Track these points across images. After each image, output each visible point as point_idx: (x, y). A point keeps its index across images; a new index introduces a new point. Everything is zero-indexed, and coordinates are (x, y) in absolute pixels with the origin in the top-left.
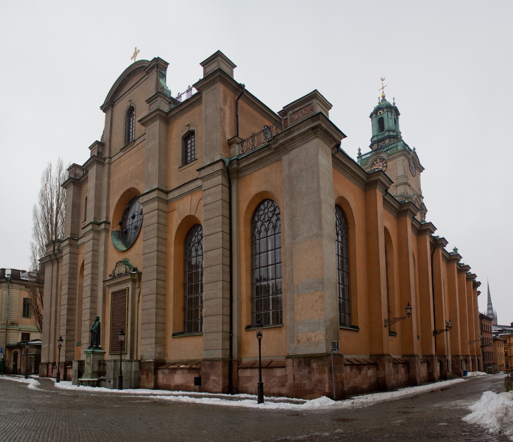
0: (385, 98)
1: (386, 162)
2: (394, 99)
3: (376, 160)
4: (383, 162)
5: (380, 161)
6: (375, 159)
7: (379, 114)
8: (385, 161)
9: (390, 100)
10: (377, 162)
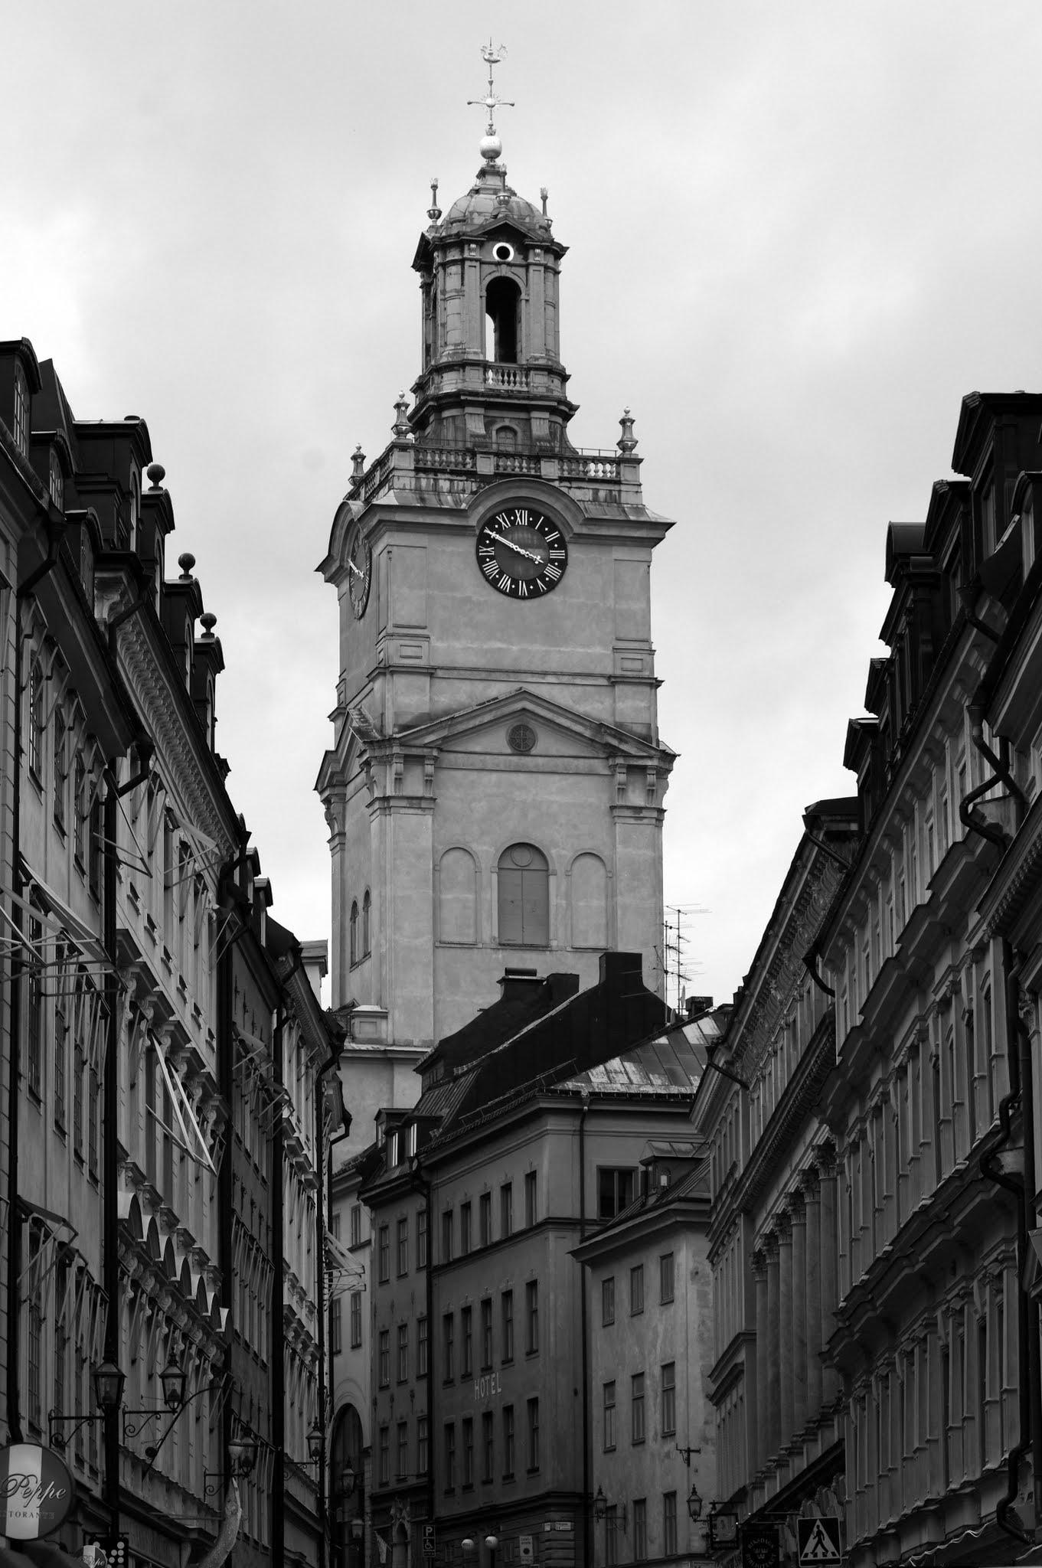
1: (562, 544)
2: (544, 198)
3: (510, 512)
4: (550, 538)
5: (531, 524)
6: (509, 505)
7: (497, 258)
8: (555, 535)
9: (525, 186)
10: (513, 523)
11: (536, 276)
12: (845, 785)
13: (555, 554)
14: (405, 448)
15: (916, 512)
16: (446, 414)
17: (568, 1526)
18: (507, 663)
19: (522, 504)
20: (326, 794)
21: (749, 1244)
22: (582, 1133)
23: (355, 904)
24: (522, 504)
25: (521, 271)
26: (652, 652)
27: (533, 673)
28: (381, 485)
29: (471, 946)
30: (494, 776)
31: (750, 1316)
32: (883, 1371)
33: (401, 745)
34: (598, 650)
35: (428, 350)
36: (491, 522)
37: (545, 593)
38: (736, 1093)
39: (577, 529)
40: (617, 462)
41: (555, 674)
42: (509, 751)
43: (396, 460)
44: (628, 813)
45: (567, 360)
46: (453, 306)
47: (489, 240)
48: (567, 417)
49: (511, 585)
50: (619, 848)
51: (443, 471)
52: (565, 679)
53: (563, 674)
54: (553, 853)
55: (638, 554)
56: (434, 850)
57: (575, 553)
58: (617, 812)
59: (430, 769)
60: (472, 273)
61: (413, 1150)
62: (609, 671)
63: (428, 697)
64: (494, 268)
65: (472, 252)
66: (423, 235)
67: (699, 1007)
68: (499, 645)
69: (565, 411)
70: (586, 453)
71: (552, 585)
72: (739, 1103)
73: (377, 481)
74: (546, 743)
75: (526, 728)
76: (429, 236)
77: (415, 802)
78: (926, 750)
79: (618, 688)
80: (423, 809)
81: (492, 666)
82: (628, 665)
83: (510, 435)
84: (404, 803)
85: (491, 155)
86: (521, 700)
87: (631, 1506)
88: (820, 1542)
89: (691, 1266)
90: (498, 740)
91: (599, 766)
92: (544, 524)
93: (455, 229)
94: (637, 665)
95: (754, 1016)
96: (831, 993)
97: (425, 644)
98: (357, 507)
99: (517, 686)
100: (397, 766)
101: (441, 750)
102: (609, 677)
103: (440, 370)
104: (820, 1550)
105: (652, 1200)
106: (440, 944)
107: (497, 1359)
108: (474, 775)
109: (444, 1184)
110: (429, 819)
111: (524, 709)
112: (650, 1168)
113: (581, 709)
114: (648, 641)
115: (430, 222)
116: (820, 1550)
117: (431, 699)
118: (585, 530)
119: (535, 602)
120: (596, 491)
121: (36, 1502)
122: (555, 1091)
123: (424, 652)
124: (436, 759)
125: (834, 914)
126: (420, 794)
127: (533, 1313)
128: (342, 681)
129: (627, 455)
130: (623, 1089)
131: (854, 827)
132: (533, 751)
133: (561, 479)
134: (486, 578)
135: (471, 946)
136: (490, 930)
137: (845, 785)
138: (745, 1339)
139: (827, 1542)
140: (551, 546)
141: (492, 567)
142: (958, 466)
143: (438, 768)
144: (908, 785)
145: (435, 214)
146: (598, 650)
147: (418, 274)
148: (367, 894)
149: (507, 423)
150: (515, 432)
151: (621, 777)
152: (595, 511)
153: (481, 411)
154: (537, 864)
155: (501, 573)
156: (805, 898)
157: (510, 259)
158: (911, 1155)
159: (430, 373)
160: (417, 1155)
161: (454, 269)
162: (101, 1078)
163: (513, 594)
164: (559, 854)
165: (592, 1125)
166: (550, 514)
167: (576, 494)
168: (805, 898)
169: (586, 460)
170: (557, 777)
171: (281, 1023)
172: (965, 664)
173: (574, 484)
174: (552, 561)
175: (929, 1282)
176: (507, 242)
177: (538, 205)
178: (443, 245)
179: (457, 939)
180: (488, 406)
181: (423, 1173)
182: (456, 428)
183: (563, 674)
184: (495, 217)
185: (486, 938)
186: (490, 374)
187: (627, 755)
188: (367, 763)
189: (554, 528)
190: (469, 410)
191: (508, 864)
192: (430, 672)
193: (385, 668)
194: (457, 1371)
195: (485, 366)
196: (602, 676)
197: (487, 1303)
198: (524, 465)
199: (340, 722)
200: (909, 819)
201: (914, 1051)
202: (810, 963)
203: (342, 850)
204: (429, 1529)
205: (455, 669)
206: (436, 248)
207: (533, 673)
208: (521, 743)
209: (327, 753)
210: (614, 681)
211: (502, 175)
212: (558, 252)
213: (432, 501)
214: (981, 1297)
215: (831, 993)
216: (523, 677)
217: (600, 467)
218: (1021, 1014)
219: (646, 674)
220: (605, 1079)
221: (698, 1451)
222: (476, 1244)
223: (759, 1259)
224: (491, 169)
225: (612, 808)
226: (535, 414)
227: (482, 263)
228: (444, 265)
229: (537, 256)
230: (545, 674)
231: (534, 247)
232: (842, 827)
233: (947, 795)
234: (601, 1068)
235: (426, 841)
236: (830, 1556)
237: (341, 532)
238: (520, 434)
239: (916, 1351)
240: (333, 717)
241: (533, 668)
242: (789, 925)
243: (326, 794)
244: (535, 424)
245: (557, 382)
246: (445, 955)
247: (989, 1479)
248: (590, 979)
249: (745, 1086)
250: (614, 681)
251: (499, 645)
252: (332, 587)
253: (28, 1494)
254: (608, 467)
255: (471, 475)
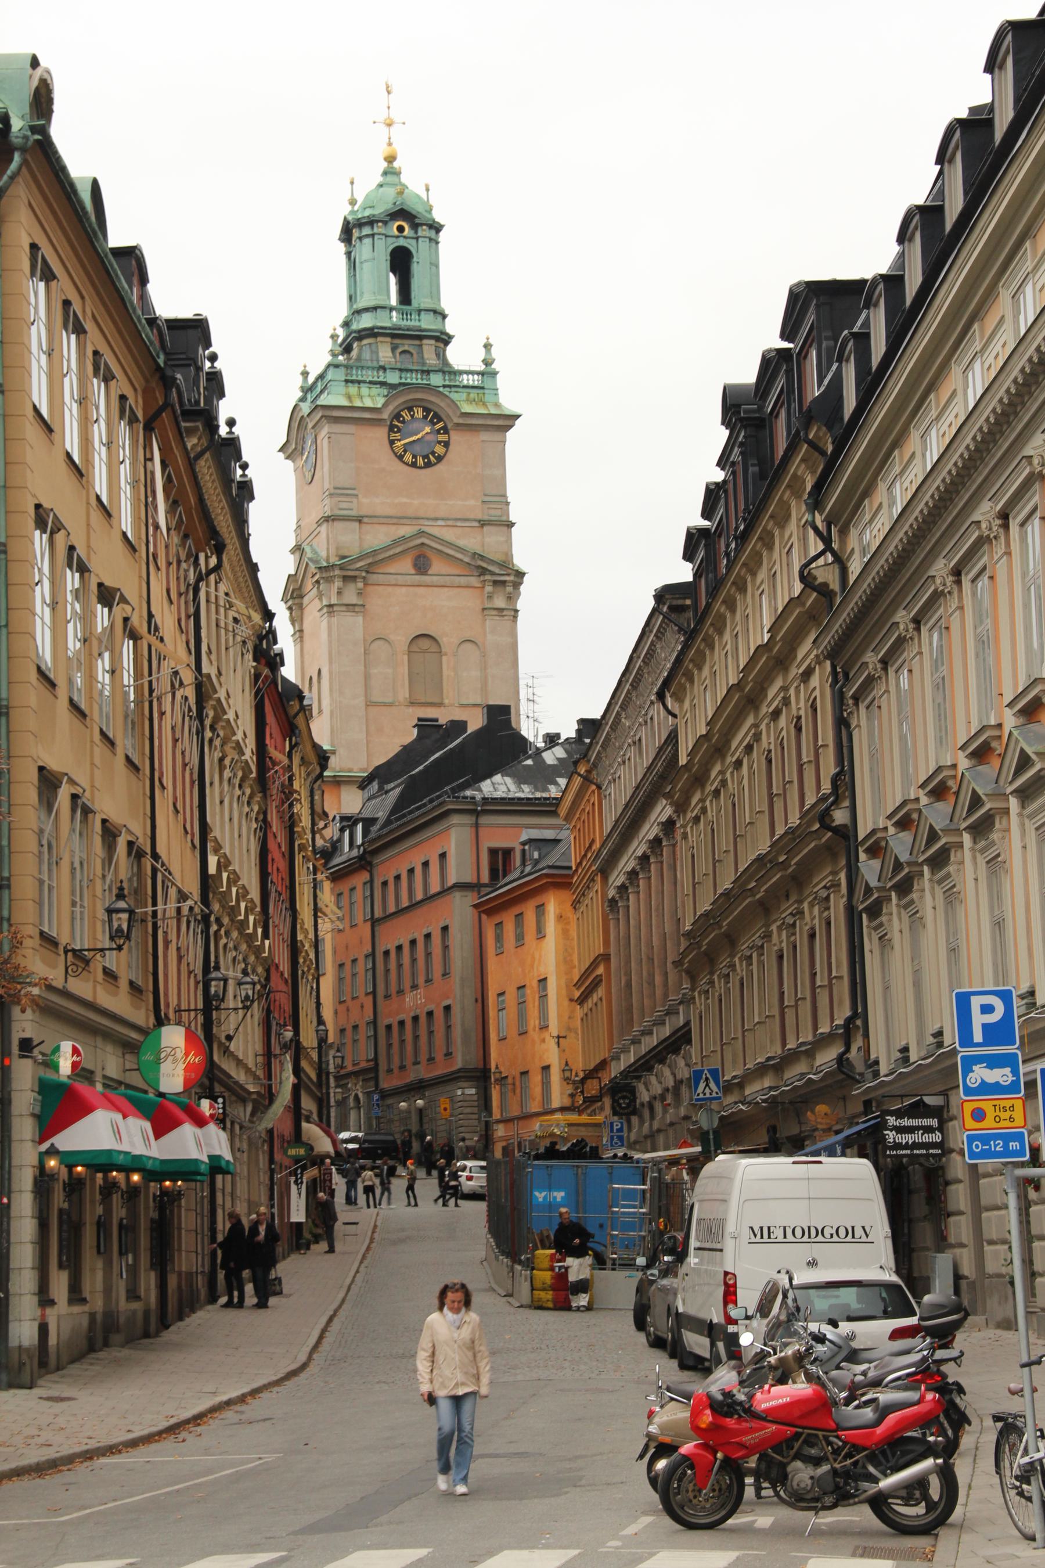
0: (396, 164)
1: (445, 430)
2: (428, 190)
3: (410, 409)
4: (438, 427)
5: (425, 417)
6: (410, 404)
7: (396, 233)
8: (441, 425)
9: (414, 181)
10: (412, 416)
11: (424, 244)
12: (684, 573)
13: (443, 438)
14: (337, 366)
15: (748, 375)
16: (365, 342)
17: (473, 1091)
18: (410, 512)
19: (418, 403)
20: (290, 603)
21: (604, 894)
22: (477, 826)
23: (311, 678)
24: (418, 403)
25: (414, 242)
26: (508, 504)
27: (428, 519)
28: (322, 392)
29: (391, 705)
30: (404, 589)
31: (607, 942)
32: (725, 971)
33: (341, 569)
34: (472, 502)
35: (351, 298)
36: (397, 416)
37: (435, 464)
38: (593, 792)
39: (456, 420)
40: (482, 374)
41: (443, 519)
42: (413, 572)
43: (329, 376)
44: (494, 613)
45: (446, 304)
46: (366, 266)
47: (391, 220)
48: (447, 343)
50: (489, 637)
51: (364, 382)
52: (450, 523)
53: (448, 519)
54: (444, 641)
55: (496, 436)
56: (365, 640)
58: (486, 612)
59: (360, 585)
60: (380, 243)
61: (359, 840)
62: (480, 517)
63: (357, 537)
64: (394, 239)
65: (379, 229)
66: (345, 218)
67: (552, 740)
68: (405, 500)
69: (444, 339)
70: (461, 368)
71: (440, 459)
72: (595, 798)
73: (319, 389)
74: (437, 566)
75: (425, 556)
76: (350, 218)
77: (350, 607)
78: (760, 538)
79: (485, 528)
80: (357, 612)
81: (399, 514)
82: (493, 512)
83: (408, 356)
84: (344, 608)
85: (391, 159)
87: (518, 1076)
88: (707, 1085)
89: (558, 911)
90: (406, 565)
91: (474, 581)
92: (433, 416)
93: (367, 213)
94: (498, 512)
95: (607, 739)
96: (675, 716)
97: (355, 500)
98: (306, 408)
99: (418, 528)
100: (338, 583)
101: (368, 572)
102: (479, 521)
103: (358, 312)
104: (707, 1091)
105: (528, 869)
106: (369, 704)
107: (421, 980)
108: (390, 589)
109: (382, 862)
110: (360, 619)
111: (423, 544)
112: (527, 847)
113: (461, 543)
114: (505, 496)
115: (350, 208)
116: (707, 1091)
117: (360, 538)
118: (461, 421)
120: (469, 394)
121: (182, 1066)
122: (458, 797)
123: (354, 505)
124: (364, 578)
125: (678, 662)
126: (354, 602)
127: (446, 947)
128: (299, 527)
129: (489, 369)
130: (504, 795)
131: (688, 602)
132: (430, 572)
133: (444, 386)
134: (395, 454)
135: (391, 705)
136: (404, 694)
137: (684, 573)
138: (605, 958)
139: (712, 1085)
140: (438, 432)
142: (785, 335)
143: (366, 584)
144: (744, 564)
145: (353, 202)
146: (472, 502)
147: (343, 245)
148: (320, 671)
149: (406, 348)
150: (411, 354)
151: (489, 588)
152: (467, 408)
153: (388, 339)
154: (434, 648)
155: (405, 451)
156: (651, 653)
157: (406, 233)
158: (748, 820)
159: (353, 314)
160: (363, 844)
161: (367, 241)
162: (196, 776)
163: (414, 465)
164: (448, 641)
165: (484, 820)
166: (437, 410)
167: (454, 396)
168: (651, 653)
169: (461, 373)
170: (446, 589)
171: (292, 747)
172: (795, 475)
173: (453, 389)
174: (439, 442)
175: (766, 908)
176: (404, 220)
177: (424, 196)
178: (360, 224)
179: (381, 700)
180: (394, 336)
181: (367, 856)
182: (372, 352)
183: (448, 519)
184: (395, 204)
185: (401, 699)
186: (394, 314)
187: (493, 574)
188: (318, 582)
189: (440, 419)
190: (379, 339)
191: (414, 648)
192: (359, 520)
193: (329, 517)
194: (393, 988)
195: (391, 309)
196: (475, 520)
197: (413, 942)
198: (419, 376)
199: (298, 555)
200: (742, 588)
201: (749, 749)
202: (661, 696)
203: (302, 641)
204: (376, 1097)
205: (376, 517)
206: (355, 226)
207: (428, 519)
208: (421, 566)
209: (289, 576)
210: (483, 523)
211: (397, 173)
212: (437, 228)
213: (358, 403)
214: (812, 916)
215: (675, 716)
216: (421, 522)
217: (470, 376)
218: (845, 715)
219: (504, 518)
220: (492, 789)
221: (565, 1037)
222: (405, 903)
223: (613, 902)
224: (391, 172)
225: (484, 609)
226: (425, 341)
227: (386, 236)
228: (360, 238)
229: (424, 231)
230: (436, 519)
231: (422, 225)
232: (680, 602)
233: (777, 567)
234: (488, 782)
235: (359, 634)
236: (714, 1095)
237: (295, 425)
238: (415, 355)
239: (755, 955)
240: (293, 551)
241: (428, 516)
242: (637, 673)
243: (290, 603)
244: (425, 348)
245: (440, 318)
246: (374, 710)
247: (822, 1042)
248: (476, 722)
249: (599, 787)
250: (483, 523)
251: (405, 500)
252: (289, 463)
253: (175, 1061)
254: (476, 377)
255: (383, 384)
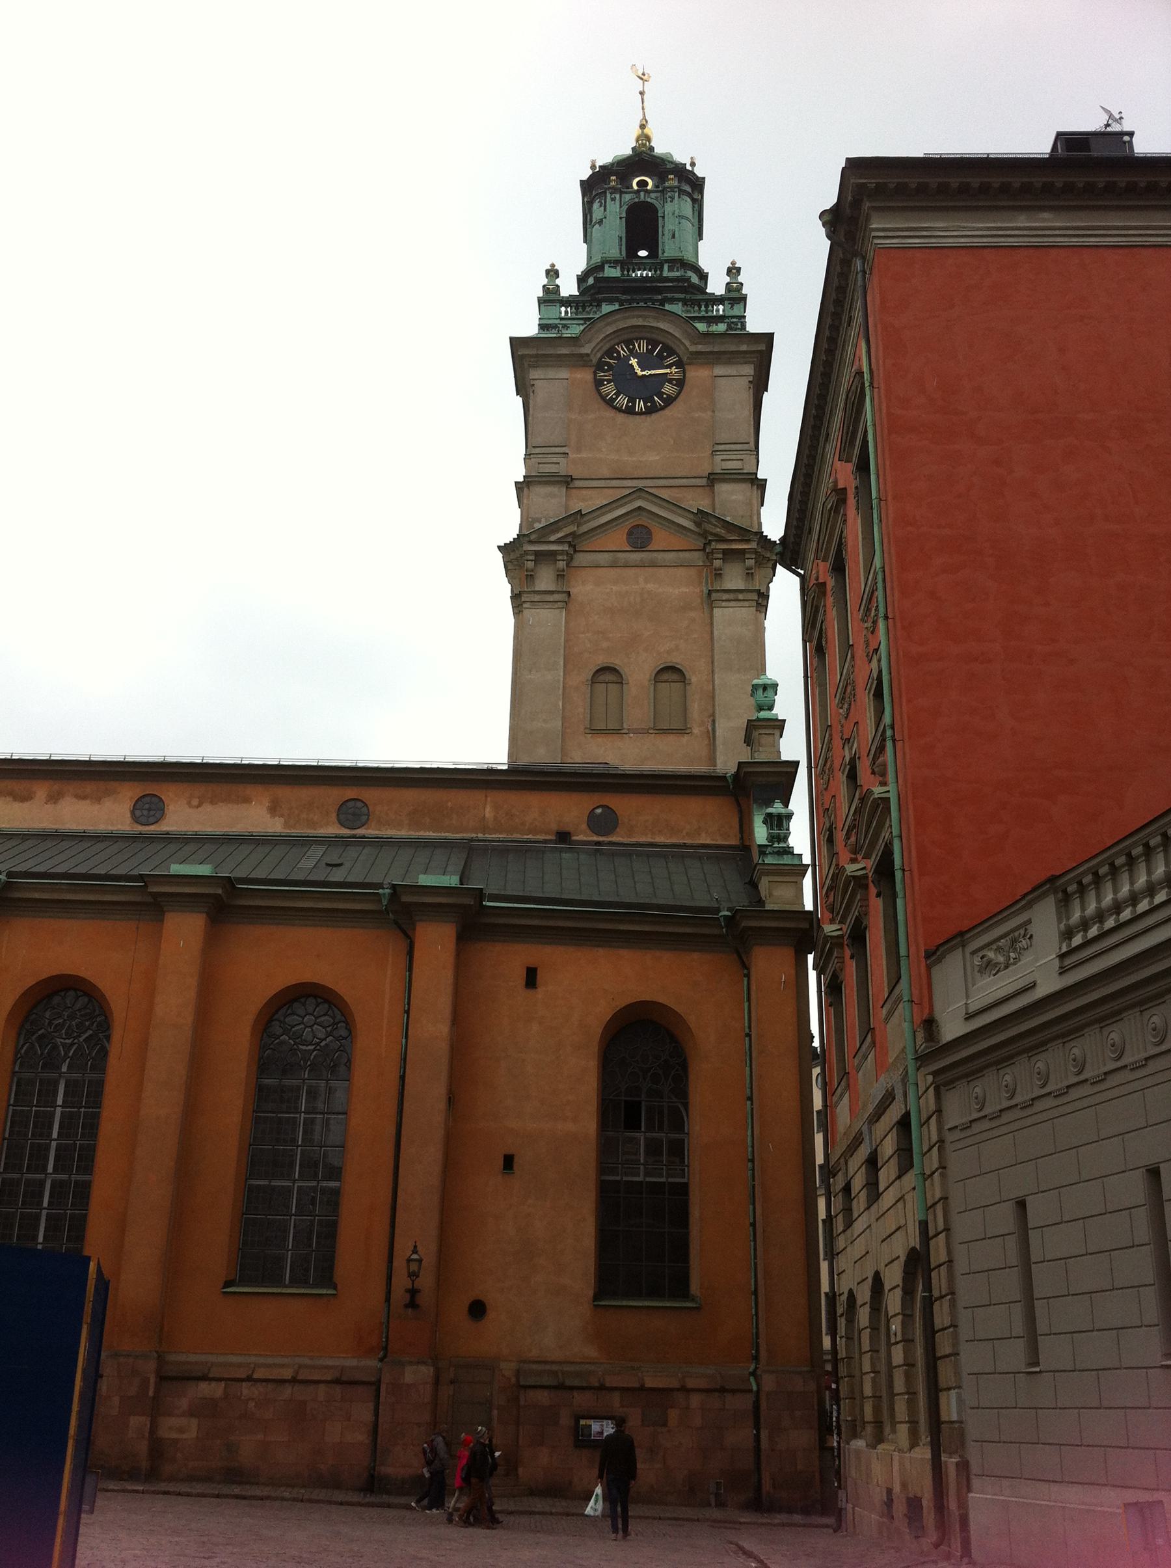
5: (650, 352)
6: (626, 337)
10: (631, 351)
36: (610, 352)
37: (662, 408)
39: (692, 348)
49: (627, 403)
57: (697, 375)
71: (669, 401)
74: (661, 538)
86: (635, 499)
111: (640, 508)
118: (700, 348)
119: (654, 416)
134: (603, 398)
141: (609, 389)
155: (617, 394)
163: (630, 411)
189: (672, 352)
